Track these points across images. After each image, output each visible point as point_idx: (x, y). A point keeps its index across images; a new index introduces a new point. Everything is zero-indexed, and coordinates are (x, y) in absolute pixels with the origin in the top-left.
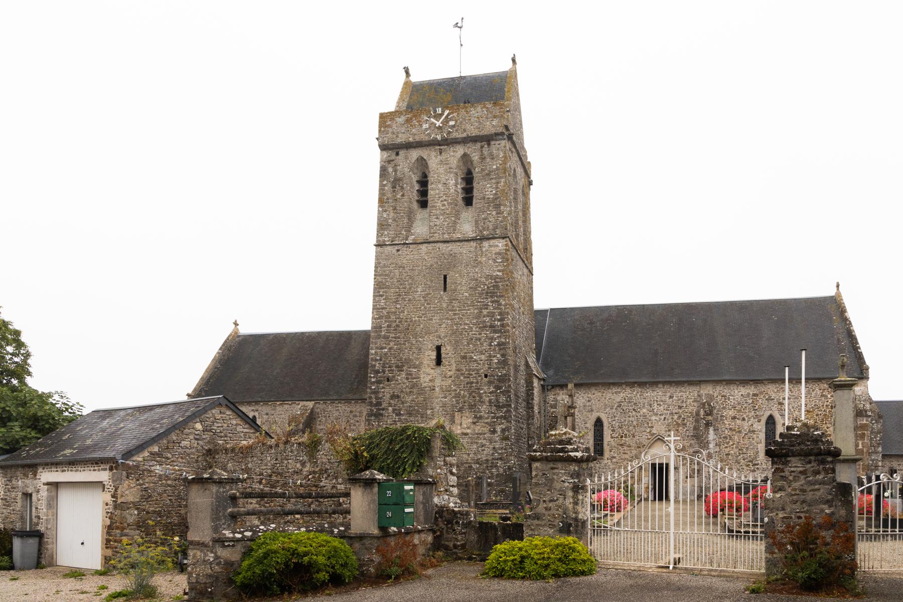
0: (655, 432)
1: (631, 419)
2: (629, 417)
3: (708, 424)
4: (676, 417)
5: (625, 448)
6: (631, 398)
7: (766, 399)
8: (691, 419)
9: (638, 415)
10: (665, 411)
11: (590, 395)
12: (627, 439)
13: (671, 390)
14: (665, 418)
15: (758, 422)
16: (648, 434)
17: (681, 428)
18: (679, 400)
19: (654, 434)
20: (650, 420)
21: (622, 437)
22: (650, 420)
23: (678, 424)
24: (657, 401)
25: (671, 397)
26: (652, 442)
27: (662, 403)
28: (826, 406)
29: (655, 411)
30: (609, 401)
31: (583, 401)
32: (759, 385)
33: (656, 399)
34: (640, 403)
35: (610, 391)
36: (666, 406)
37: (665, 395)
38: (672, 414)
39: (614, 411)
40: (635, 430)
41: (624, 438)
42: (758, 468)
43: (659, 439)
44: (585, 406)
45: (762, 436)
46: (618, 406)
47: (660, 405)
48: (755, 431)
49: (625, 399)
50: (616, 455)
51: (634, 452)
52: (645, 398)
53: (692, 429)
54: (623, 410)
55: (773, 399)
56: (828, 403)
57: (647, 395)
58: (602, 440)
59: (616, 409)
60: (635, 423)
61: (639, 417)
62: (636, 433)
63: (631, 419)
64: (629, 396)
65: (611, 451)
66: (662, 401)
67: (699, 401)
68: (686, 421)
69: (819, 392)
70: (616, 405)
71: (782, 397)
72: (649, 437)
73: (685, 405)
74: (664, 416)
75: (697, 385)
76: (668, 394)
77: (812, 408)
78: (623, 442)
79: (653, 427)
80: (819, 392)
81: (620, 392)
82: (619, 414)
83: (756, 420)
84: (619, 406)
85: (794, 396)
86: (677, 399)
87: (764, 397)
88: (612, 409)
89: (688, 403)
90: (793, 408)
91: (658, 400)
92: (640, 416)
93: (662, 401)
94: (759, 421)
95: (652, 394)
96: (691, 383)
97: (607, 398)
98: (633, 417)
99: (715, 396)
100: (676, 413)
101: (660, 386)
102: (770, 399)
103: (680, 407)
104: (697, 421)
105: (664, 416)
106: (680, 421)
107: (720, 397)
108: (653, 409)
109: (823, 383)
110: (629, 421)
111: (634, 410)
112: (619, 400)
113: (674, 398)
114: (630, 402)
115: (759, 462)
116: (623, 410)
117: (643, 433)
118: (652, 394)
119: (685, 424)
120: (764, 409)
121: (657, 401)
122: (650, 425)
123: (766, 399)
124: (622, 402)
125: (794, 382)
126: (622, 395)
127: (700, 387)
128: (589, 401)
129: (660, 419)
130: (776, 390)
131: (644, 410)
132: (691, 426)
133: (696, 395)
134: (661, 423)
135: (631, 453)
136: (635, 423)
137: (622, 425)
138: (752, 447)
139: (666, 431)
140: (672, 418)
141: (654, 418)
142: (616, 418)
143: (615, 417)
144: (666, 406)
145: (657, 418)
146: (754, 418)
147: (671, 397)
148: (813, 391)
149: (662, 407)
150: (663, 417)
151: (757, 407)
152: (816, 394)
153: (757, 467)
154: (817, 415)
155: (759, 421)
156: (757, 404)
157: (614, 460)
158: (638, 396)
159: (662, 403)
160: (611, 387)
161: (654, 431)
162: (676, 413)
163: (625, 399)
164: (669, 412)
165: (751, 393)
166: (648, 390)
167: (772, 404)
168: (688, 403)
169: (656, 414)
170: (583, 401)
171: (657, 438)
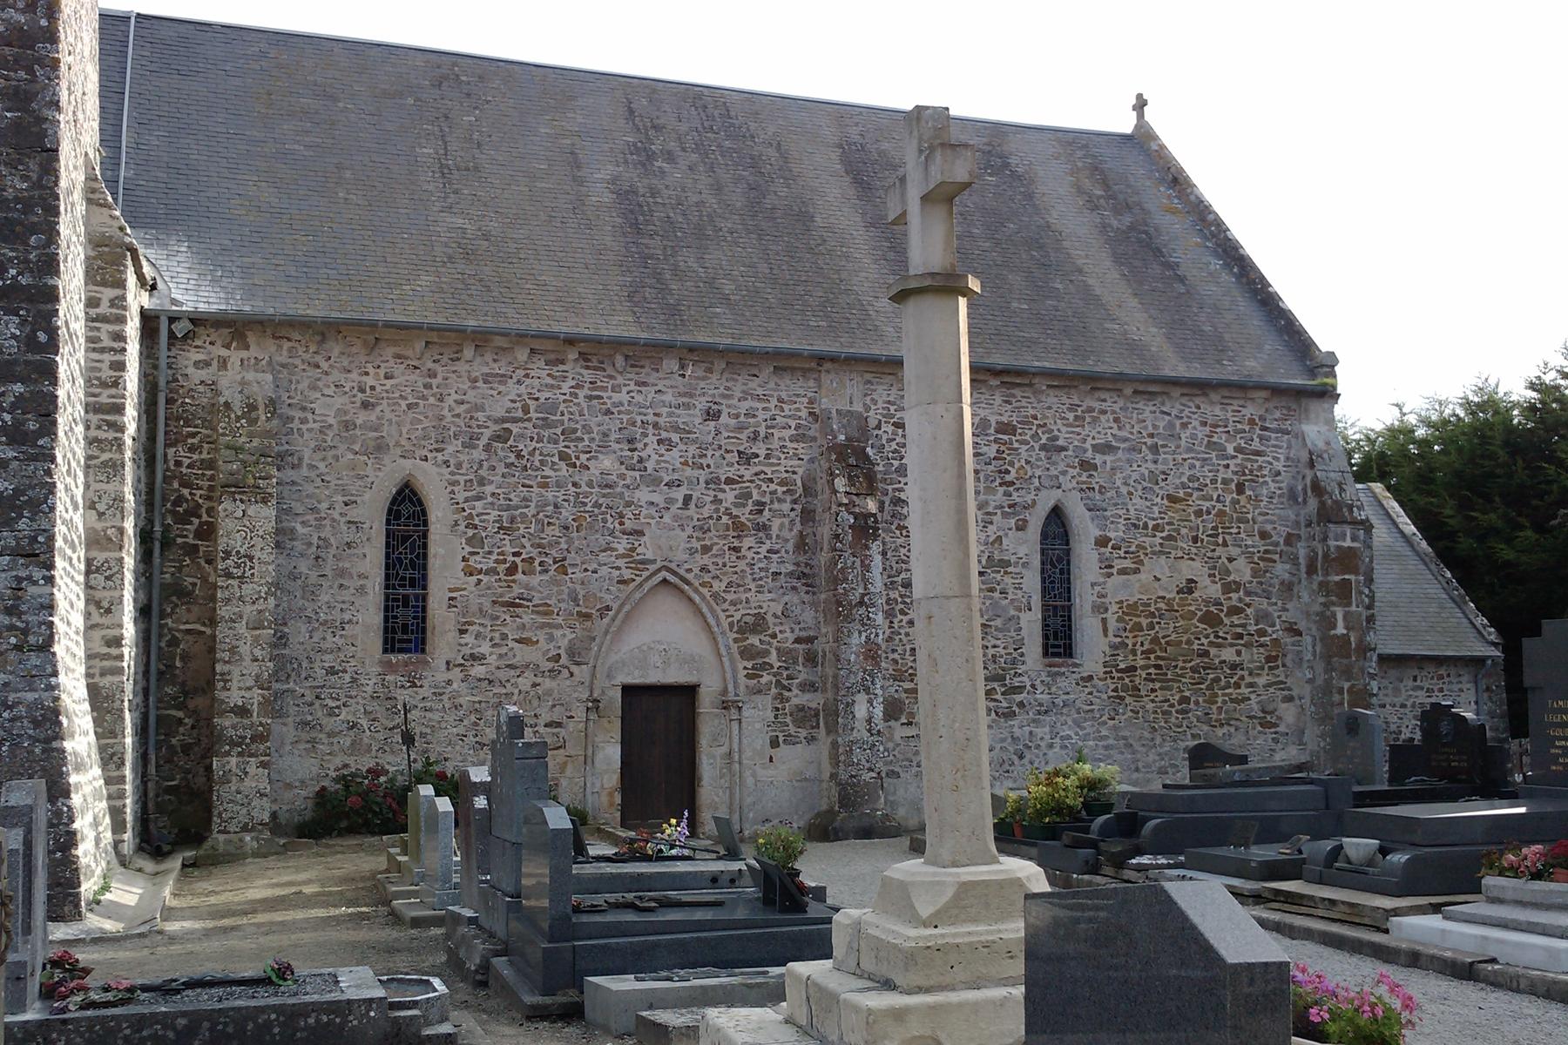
0: (650, 556)
1: (550, 495)
2: (544, 485)
3: (865, 529)
4: (729, 496)
5: (526, 619)
6: (552, 408)
7: (1043, 448)
8: (786, 507)
9: (582, 478)
10: (688, 471)
11: (370, 381)
12: (535, 580)
13: (713, 385)
14: (687, 499)
15: (1018, 529)
16: (621, 563)
17: (748, 542)
18: (741, 428)
19: (642, 562)
20: (628, 504)
21: (512, 570)
22: (628, 504)
23: (738, 527)
24: (656, 425)
25: (711, 415)
26: (638, 595)
27: (675, 437)
28: (1225, 482)
29: (650, 465)
30: (461, 409)
31: (339, 401)
32: (1017, 392)
33: (651, 418)
34: (587, 429)
35: (462, 367)
36: (692, 449)
37: (687, 406)
38: (713, 481)
39: (478, 454)
40: (570, 541)
41: (519, 576)
42: (1021, 705)
43: (665, 581)
44: (348, 426)
45: (1032, 582)
46: (497, 438)
47: (670, 445)
48: (1008, 563)
49: (526, 410)
50: (485, 648)
51: (564, 638)
52: (608, 412)
53: (790, 546)
54: (519, 456)
55: (1064, 449)
56: (1229, 475)
57: (616, 397)
58: (421, 581)
59: (487, 448)
60: (567, 513)
61: (585, 488)
62: (572, 558)
63: (550, 495)
64: (543, 396)
65: (462, 632)
66: (676, 429)
67: (814, 439)
68: (766, 513)
69: (1202, 432)
70: (487, 433)
71: (1090, 441)
72: (627, 574)
73: (762, 453)
74: (683, 491)
75: (805, 372)
76: (701, 404)
77: (1184, 486)
78: (517, 590)
79: (640, 533)
80: (1202, 432)
81: (503, 379)
82: (501, 469)
83: (1013, 521)
84: (503, 436)
85: (1126, 440)
86: (733, 422)
87: (1035, 436)
88: (470, 445)
89: (776, 444)
90: (1126, 484)
91: (661, 421)
92: (590, 484)
93: (676, 429)
94: (1021, 527)
95: (639, 398)
96: (785, 362)
97: (450, 401)
98: (559, 485)
99: (872, 423)
100: (729, 481)
101: (671, 364)
102: (1052, 448)
103: (746, 458)
104: (808, 515)
105: (683, 491)
106: (744, 515)
107: (890, 429)
108: (641, 461)
109: (1212, 403)
110: (542, 506)
111: (563, 457)
112: (500, 413)
113: (724, 419)
114: (546, 424)
115: (1025, 679)
116: (519, 456)
117: (603, 557)
118: (639, 398)
119: (764, 528)
120: (1036, 481)
121: (656, 425)
122: (629, 525)
123: (1043, 448)
124: (515, 420)
125: (1128, 391)
126: (512, 389)
127: (818, 380)
128: (366, 405)
129: (670, 501)
130: (1071, 416)
131: (607, 462)
132: (786, 534)
133: (804, 413)
134: (676, 518)
135: (551, 638)
136: (567, 513)
137: (512, 520)
138: (998, 622)
139: (692, 552)
140: (716, 501)
141: (643, 495)
142: (489, 489)
143: (482, 482)
144: (692, 449)
145: (657, 498)
146: (1005, 515)
147: (711, 415)
148: (1184, 426)
149: (675, 453)
150: (679, 494)
151: (1013, 471)
152: (1194, 437)
153: (1018, 698)
154: (1199, 513)
155: (1021, 527)
156: (1012, 464)
157: (478, 670)
158: (581, 399)
159: (675, 437)
160: (468, 352)
161: (647, 550)
162: (729, 481)
163: (526, 410)
164: (703, 475)
165: (993, 419)
166: (620, 380)
167: (1061, 467)
168: (776, 444)
169: (655, 482)
170: (339, 401)
171: (659, 577)
